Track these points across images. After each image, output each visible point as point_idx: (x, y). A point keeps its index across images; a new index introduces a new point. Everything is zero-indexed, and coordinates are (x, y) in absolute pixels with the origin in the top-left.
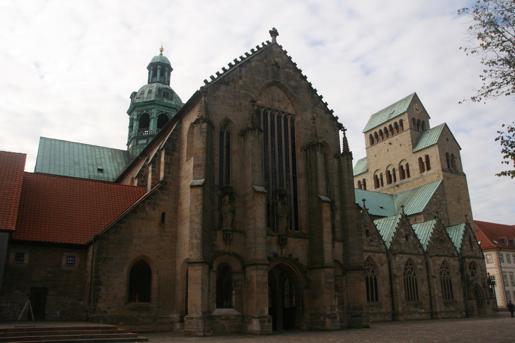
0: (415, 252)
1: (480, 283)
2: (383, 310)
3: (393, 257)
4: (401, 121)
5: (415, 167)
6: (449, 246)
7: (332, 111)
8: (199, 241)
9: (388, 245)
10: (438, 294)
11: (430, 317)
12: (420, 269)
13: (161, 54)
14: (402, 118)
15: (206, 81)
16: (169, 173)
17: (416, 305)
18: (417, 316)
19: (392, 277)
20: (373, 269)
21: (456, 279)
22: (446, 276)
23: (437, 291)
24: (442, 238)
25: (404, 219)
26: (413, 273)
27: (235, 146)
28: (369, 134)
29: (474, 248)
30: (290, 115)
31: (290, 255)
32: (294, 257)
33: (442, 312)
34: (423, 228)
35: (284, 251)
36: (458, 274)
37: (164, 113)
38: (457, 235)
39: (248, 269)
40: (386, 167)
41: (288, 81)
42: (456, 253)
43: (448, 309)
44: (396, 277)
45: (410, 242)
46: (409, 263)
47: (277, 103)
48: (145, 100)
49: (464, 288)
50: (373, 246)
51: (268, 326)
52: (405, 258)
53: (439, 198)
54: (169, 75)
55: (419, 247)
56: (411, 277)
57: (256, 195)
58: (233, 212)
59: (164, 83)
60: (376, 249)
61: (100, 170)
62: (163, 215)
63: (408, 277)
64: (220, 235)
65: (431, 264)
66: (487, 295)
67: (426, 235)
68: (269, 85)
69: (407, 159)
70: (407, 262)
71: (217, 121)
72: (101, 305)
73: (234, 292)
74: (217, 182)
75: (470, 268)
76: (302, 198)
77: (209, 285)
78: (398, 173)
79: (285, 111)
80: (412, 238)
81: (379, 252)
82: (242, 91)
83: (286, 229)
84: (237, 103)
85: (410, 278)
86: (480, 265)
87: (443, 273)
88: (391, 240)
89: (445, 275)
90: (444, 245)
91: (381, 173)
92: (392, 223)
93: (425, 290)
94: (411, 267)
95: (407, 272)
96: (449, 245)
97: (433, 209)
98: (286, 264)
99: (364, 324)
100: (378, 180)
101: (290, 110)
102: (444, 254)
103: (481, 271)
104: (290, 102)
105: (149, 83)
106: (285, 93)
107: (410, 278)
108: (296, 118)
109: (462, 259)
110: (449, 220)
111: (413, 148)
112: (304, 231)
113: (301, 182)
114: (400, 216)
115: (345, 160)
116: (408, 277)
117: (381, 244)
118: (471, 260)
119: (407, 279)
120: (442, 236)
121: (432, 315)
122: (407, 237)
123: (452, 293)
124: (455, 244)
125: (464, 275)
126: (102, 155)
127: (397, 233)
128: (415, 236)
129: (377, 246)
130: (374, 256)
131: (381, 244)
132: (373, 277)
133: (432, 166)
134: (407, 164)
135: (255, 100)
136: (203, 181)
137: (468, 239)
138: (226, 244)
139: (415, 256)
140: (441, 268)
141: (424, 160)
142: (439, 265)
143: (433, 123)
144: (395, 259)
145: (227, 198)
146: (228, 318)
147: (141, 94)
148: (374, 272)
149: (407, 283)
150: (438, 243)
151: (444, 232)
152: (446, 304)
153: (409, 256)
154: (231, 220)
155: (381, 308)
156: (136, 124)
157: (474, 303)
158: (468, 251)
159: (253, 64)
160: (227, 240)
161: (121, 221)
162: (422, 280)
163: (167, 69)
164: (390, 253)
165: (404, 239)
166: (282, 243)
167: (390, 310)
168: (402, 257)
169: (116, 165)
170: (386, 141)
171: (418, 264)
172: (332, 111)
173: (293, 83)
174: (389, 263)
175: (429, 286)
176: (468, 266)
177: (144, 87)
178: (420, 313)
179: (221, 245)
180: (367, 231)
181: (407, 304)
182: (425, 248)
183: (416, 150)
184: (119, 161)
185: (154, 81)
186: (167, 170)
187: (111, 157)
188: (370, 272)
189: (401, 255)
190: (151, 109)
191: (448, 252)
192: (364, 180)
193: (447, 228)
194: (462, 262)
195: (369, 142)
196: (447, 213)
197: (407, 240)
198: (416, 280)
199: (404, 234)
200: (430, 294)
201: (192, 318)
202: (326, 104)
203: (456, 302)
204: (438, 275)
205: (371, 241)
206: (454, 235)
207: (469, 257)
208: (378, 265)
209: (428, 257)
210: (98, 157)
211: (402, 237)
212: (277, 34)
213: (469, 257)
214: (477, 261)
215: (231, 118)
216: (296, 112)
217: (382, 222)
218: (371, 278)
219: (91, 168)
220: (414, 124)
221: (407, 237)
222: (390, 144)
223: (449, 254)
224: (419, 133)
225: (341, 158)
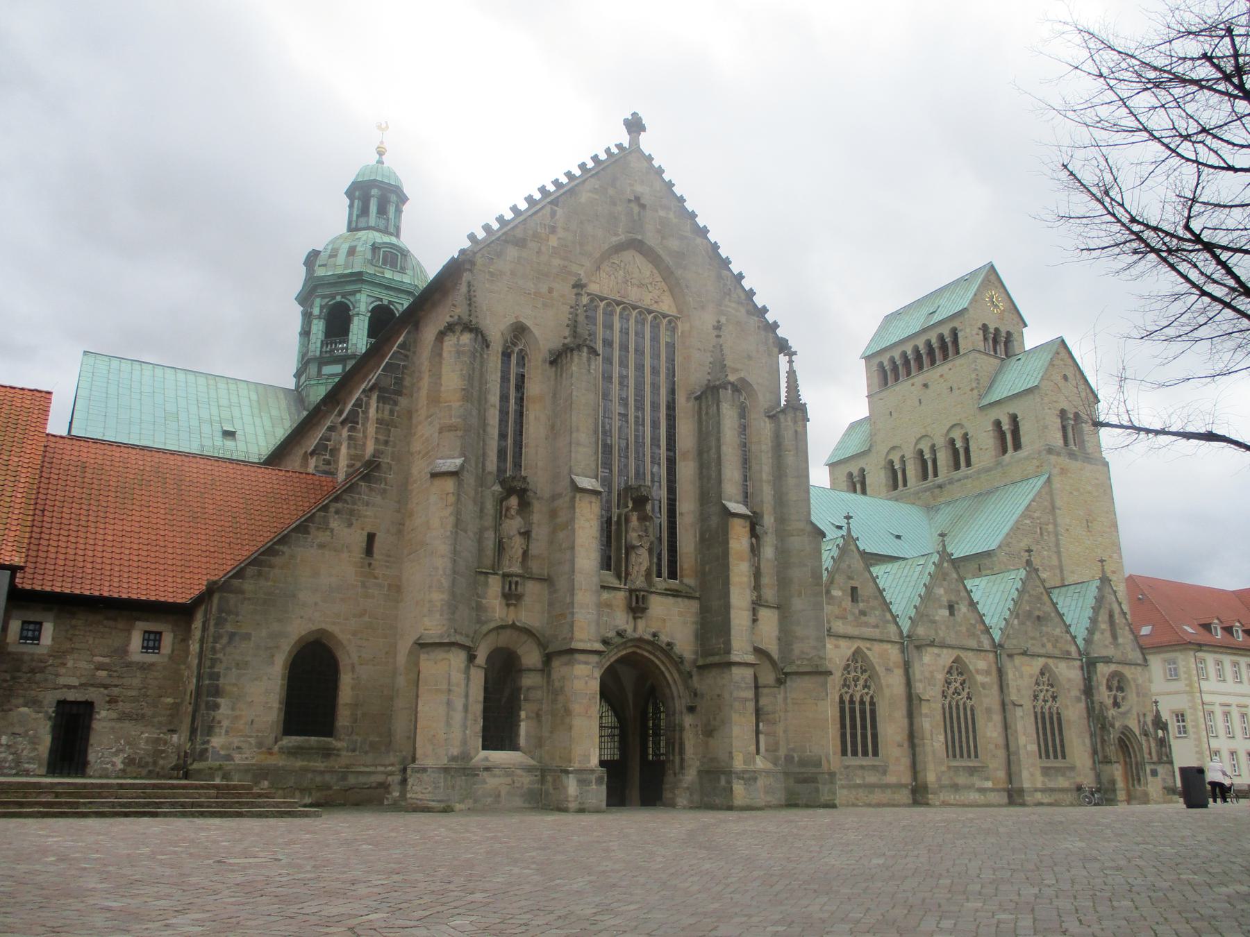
0: (973, 643)
1: (1134, 725)
2: (891, 779)
3: (915, 653)
4: (954, 333)
5: (983, 443)
6: (1057, 631)
7: (765, 310)
8: (445, 596)
9: (906, 626)
10: (1025, 746)
11: (1006, 800)
12: (983, 685)
13: (380, 162)
14: (956, 324)
15: (472, 237)
16: (386, 443)
17: (972, 771)
18: (974, 796)
19: (912, 701)
20: (866, 681)
21: (1074, 713)
22: (1049, 704)
23: (1022, 740)
24: (1040, 614)
25: (945, 565)
26: (964, 694)
27: (534, 388)
28: (876, 361)
29: (1120, 640)
30: (665, 316)
31: (655, 635)
32: (664, 639)
33: (1036, 790)
34: (995, 589)
35: (641, 624)
36: (1079, 700)
37: (386, 302)
38: (1076, 610)
39: (556, 663)
40: (914, 441)
41: (663, 238)
42: (1073, 649)
43: (1052, 785)
44: (921, 700)
46: (958, 667)
47: (635, 289)
48: (339, 271)
49: (1092, 735)
50: (866, 624)
51: (599, 793)
52: (947, 657)
54: (399, 211)
55: (982, 632)
56: (961, 703)
57: (578, 496)
58: (526, 534)
59: (385, 231)
60: (875, 633)
61: (229, 434)
62: (371, 538)
63: (954, 703)
64: (495, 586)
65: (1011, 675)
66: (1150, 754)
67: (1002, 603)
69: (965, 422)
70: (951, 668)
71: (496, 330)
72: (217, 741)
73: (523, 714)
74: (492, 464)
75: (1110, 688)
76: (687, 507)
77: (467, 696)
78: (943, 458)
79: (654, 307)
81: (882, 641)
82: (557, 262)
83: (648, 574)
84: (544, 289)
85: (957, 705)
86: (1135, 680)
87: (1041, 696)
88: (912, 613)
89: (1045, 701)
90: (1044, 628)
91: (903, 456)
92: (916, 574)
93: (995, 735)
94: (960, 679)
95: (952, 690)
96: (1058, 630)
98: (646, 654)
99: (825, 798)
100: (894, 472)
101: (667, 306)
102: (1042, 651)
103: (1138, 695)
104: (666, 288)
105: (350, 229)
106: (657, 266)
107: (957, 705)
108: (679, 324)
109: (1090, 665)
110: (1062, 571)
111: (980, 397)
112: (690, 581)
113: (687, 471)
114: (936, 558)
115: (790, 423)
116: (954, 703)
117: (888, 622)
118: (1113, 667)
119: (950, 707)
120: (1039, 609)
121: (1010, 796)
123: (1062, 746)
124: (1072, 629)
125: (1092, 703)
126: (234, 399)
127: (928, 596)
128: (973, 605)
129: (877, 626)
130: (869, 649)
131: (888, 622)
132: (867, 699)
133: (1023, 440)
134: (966, 434)
135: (584, 281)
136: (459, 461)
137: (1106, 617)
138: (508, 605)
139: (970, 654)
140: (1037, 684)
141: (1006, 427)
142: (1031, 676)
143: (1032, 338)
144: (921, 659)
145: (514, 501)
146: (507, 771)
147: (331, 256)
148: (869, 688)
149: (951, 718)
150: (1029, 623)
151: (1045, 598)
152: (1046, 771)
153: (956, 653)
154: (520, 552)
155: (885, 773)
156: (318, 327)
157: (1117, 772)
158: (1106, 646)
159: (584, 197)
160: (511, 597)
161: (270, 551)
162: (989, 711)
163: (393, 198)
164: (911, 645)
165: (947, 613)
166: (637, 607)
167: (906, 779)
168: (939, 655)
169: (268, 423)
170: (915, 380)
171: (977, 671)
172: (765, 310)
173: (674, 244)
174: (907, 667)
175: (1006, 727)
176: (1105, 682)
177: (336, 238)
178: (982, 790)
179: (497, 610)
180: (854, 589)
181: (949, 768)
182: (997, 636)
183: (985, 402)
184: (275, 413)
185: (360, 225)
186: (381, 438)
187: (255, 404)
188: (859, 688)
189: (936, 650)
190: (354, 293)
191: (1054, 646)
192: (862, 470)
193: (1057, 591)
194: (1089, 672)
195: (876, 380)
196: (1058, 553)
197: (952, 614)
198: (972, 710)
199: (945, 600)
200: (1007, 746)
201: (424, 770)
202: (751, 293)
203: (1072, 768)
204: (1027, 703)
205: (863, 613)
206: (1073, 608)
207: (1107, 660)
208: (880, 670)
209: (1004, 657)
210: (224, 402)
211: (940, 607)
212: (643, 128)
213: (1107, 660)
214: (1128, 672)
215: (528, 323)
216: (680, 311)
217: (893, 571)
218: (862, 702)
219: (206, 429)
220: (985, 339)
221: (951, 608)
222: (926, 386)
223: (1057, 652)
224: (997, 361)
225: (782, 417)
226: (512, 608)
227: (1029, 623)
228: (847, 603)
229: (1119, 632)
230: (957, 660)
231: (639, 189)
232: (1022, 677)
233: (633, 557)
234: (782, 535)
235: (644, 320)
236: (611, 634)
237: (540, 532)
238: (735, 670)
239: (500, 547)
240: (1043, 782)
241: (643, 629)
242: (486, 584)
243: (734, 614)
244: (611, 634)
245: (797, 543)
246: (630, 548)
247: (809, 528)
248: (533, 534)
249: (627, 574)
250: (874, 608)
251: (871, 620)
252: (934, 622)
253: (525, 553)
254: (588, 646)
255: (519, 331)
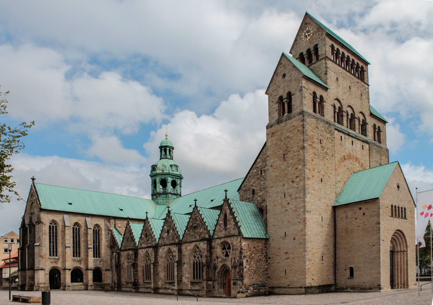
18: (170, 291)
24: (196, 225)
45: (170, 235)
46: (169, 251)
53: (260, 166)
80: (171, 231)
86: (232, 244)
90: (197, 231)
96: (202, 230)
97: (251, 183)
102: (195, 240)
118: (223, 240)
120: (195, 223)
122: (168, 232)
139: (172, 246)
142: (190, 250)
158: (221, 231)
165: (166, 234)
189: (163, 247)
191: (200, 237)
197: (168, 234)
199: (166, 230)
221: (168, 232)
227: (191, 230)
228: (145, 239)
229: (228, 222)
230: (169, 249)
232: (187, 251)
240: (191, 287)
250: (150, 238)
251: (149, 242)
252: (163, 238)
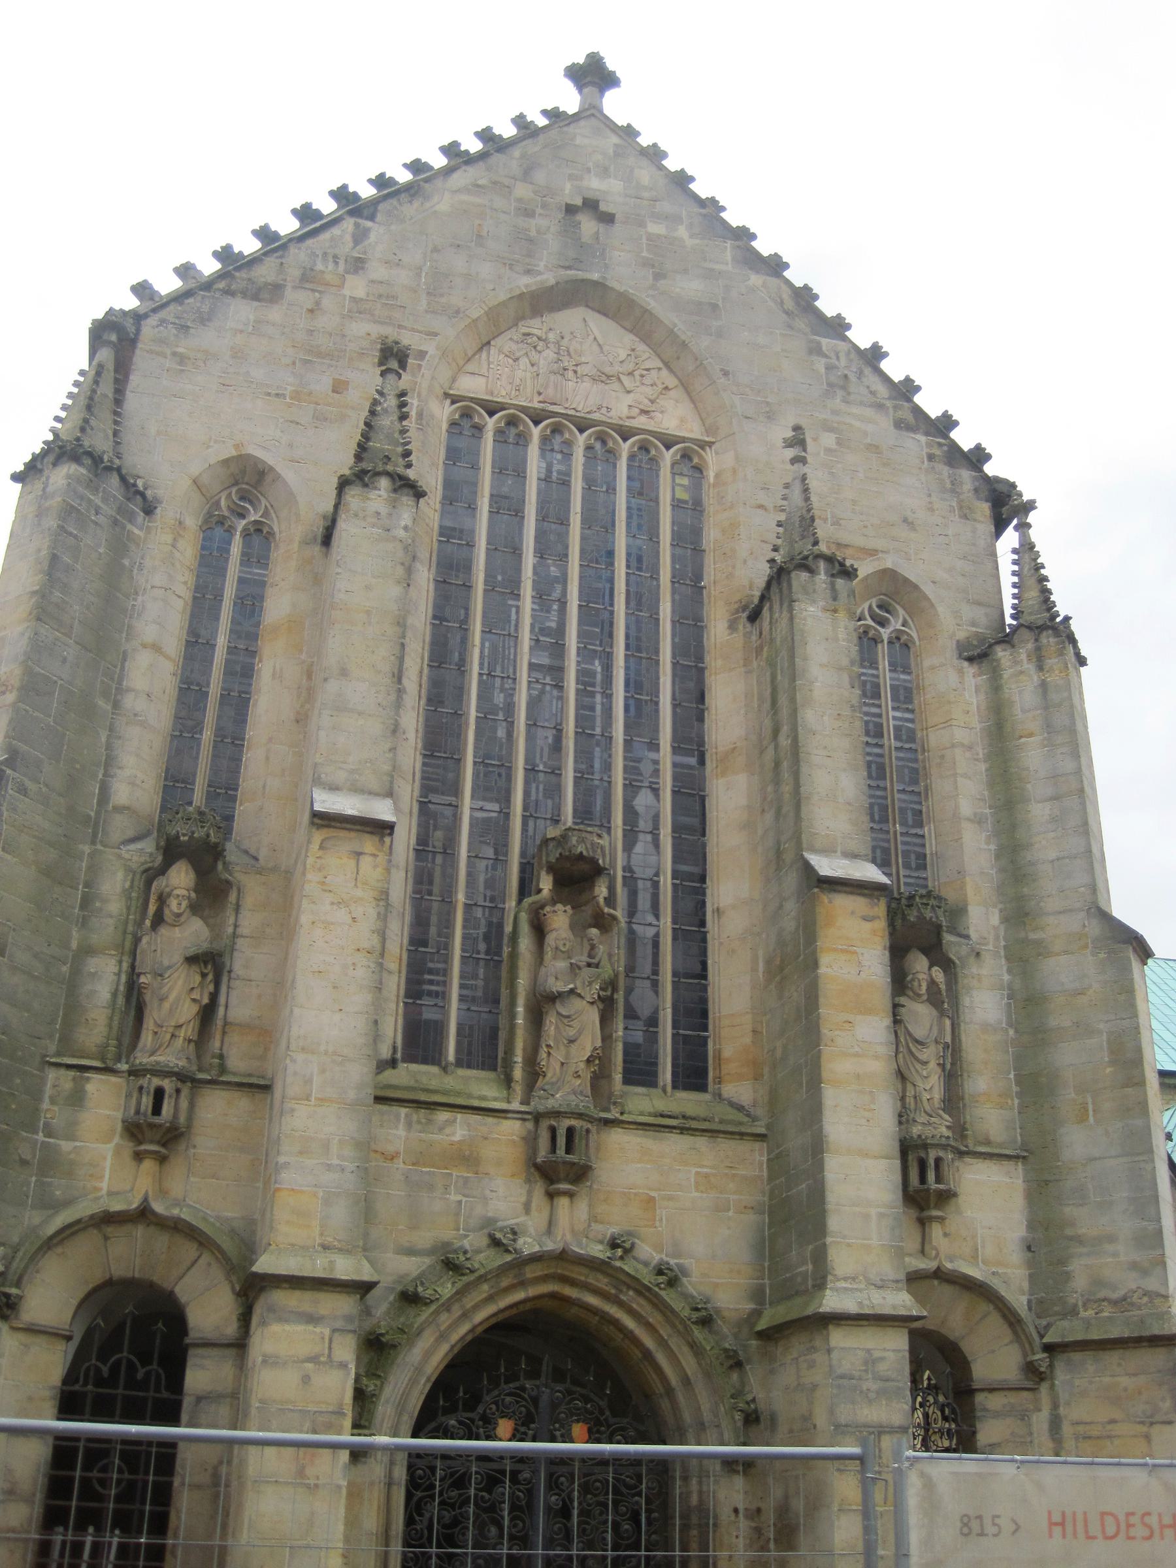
7: (947, 423)
15: (142, 289)
32: (648, 1252)
41: (658, 276)
47: (587, 384)
64: (106, 1102)
68: (541, 302)
76: (733, 890)
79: (641, 422)
83: (599, 1065)
84: (321, 383)
98: (592, 1300)
101: (675, 418)
104: (672, 381)
108: (710, 456)
112: (740, 1090)
113: (730, 797)
145: (181, 878)
166: (559, 1167)
172: (947, 423)
173: (691, 287)
202: (908, 388)
215: (269, 458)
226: (148, 1165)
231: (595, 184)
233: (551, 1023)
234: (1023, 955)
235: (611, 455)
236: (475, 1241)
237: (250, 962)
238: (838, 1338)
239: (134, 1002)
241: (576, 1226)
242: (77, 1099)
243: (834, 1168)
244: (475, 1241)
245: (1068, 970)
246: (543, 1003)
247: (1094, 928)
248: (238, 965)
249: (534, 1073)
253: (207, 1014)
254: (317, 1267)
255: (247, 479)
